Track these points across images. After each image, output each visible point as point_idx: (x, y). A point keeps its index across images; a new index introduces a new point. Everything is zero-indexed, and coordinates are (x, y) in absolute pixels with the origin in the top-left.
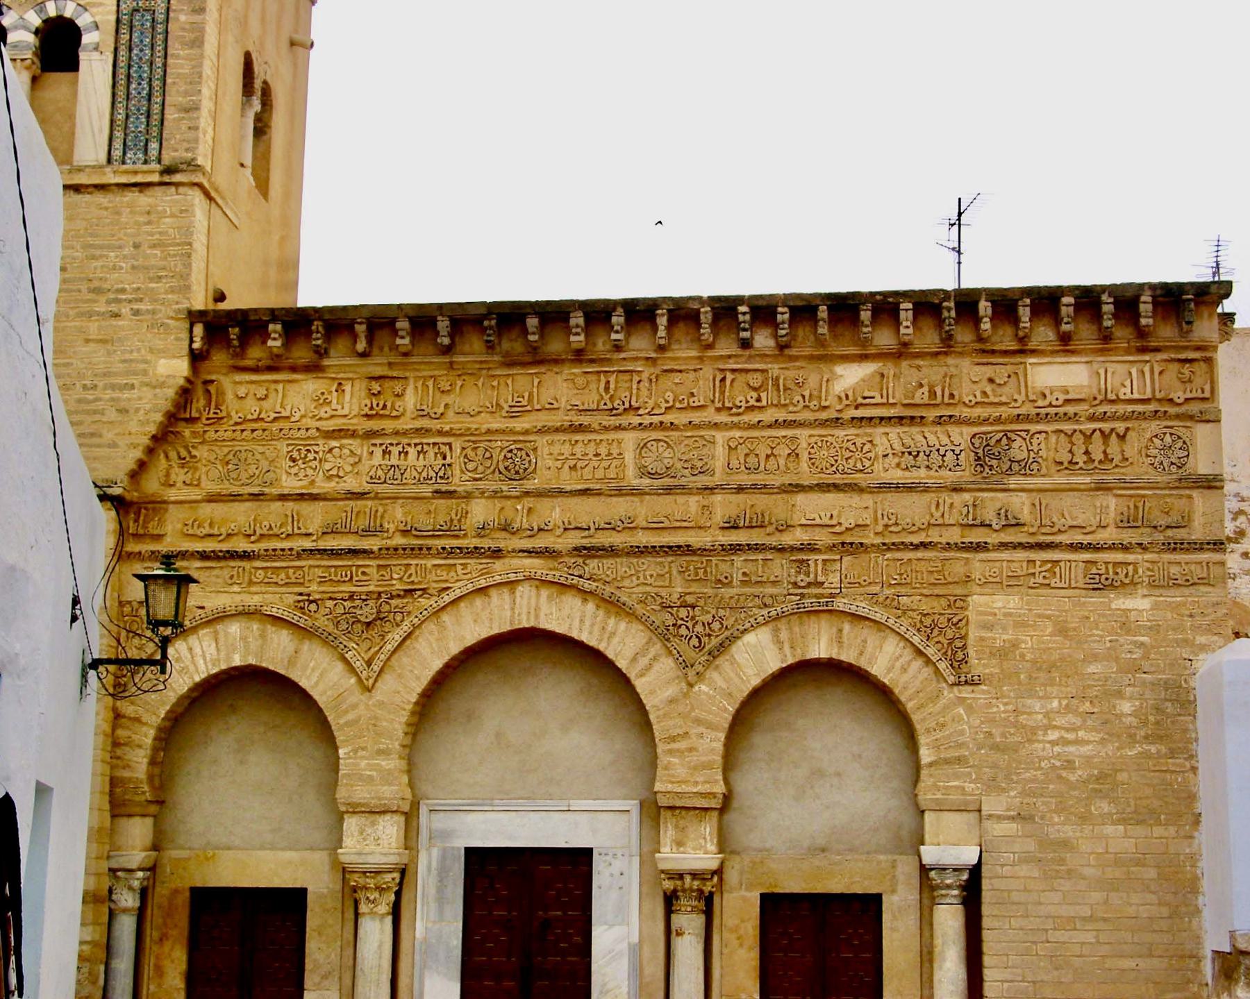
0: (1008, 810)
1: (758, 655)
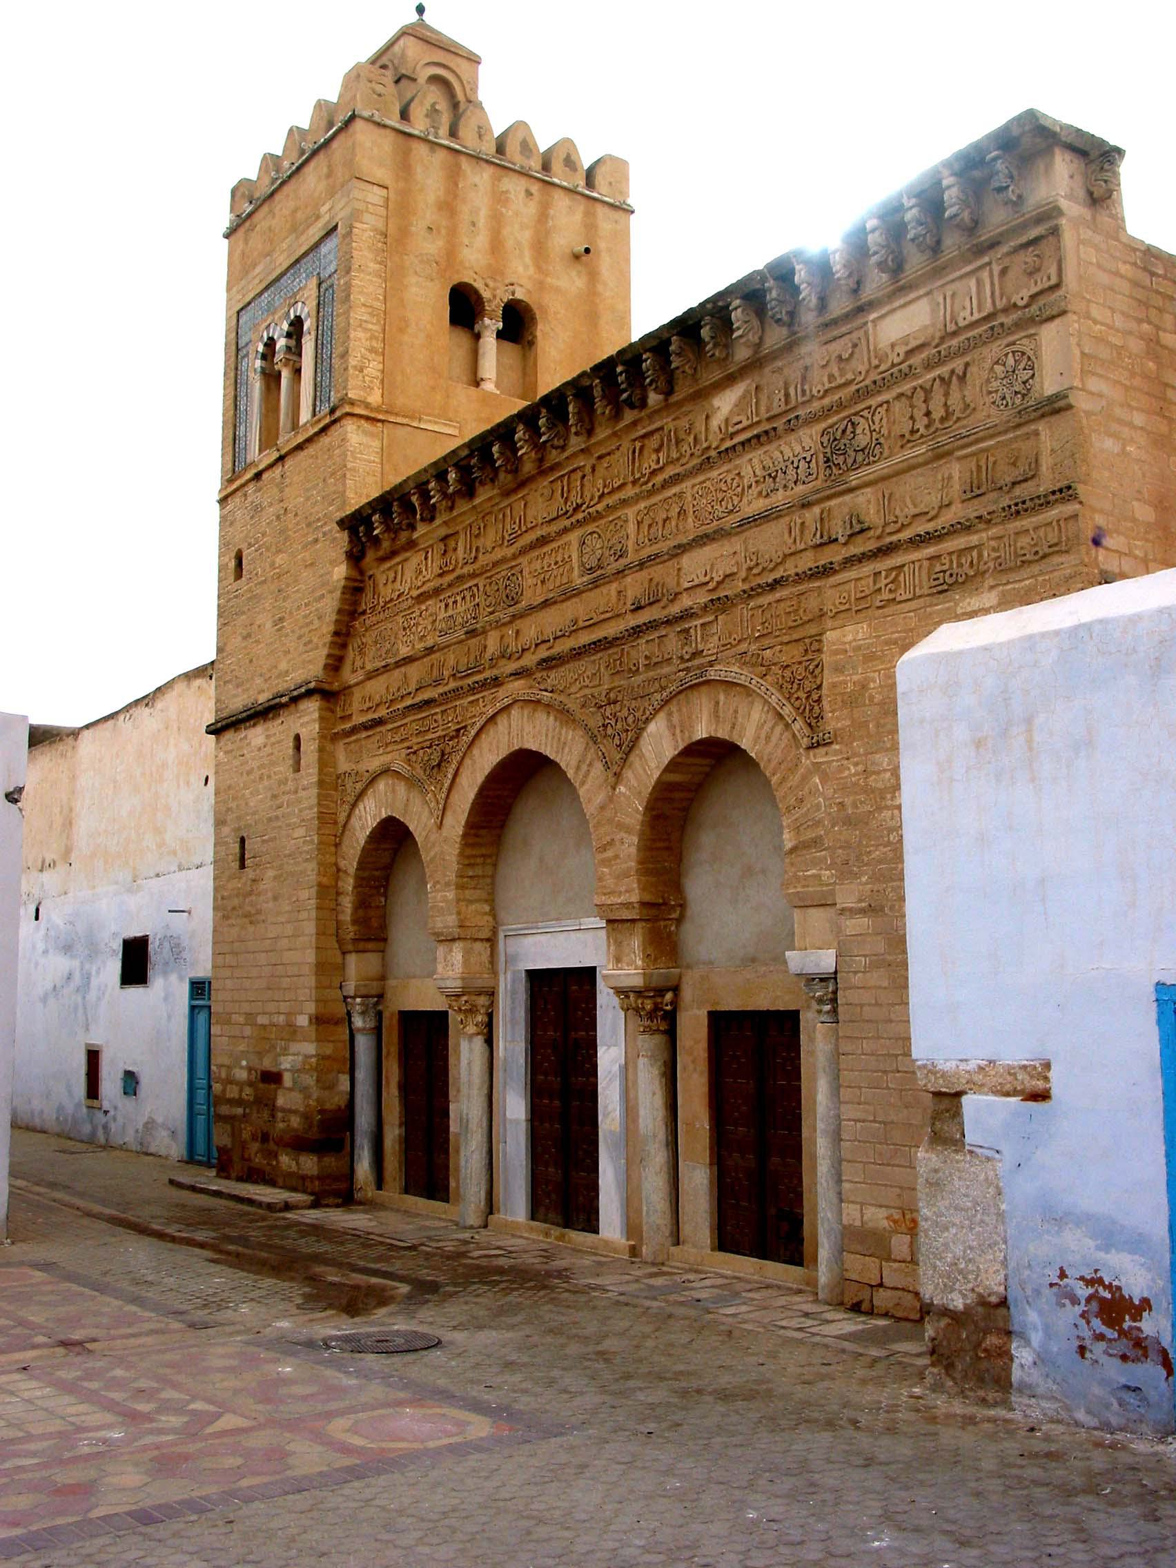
0: (860, 901)
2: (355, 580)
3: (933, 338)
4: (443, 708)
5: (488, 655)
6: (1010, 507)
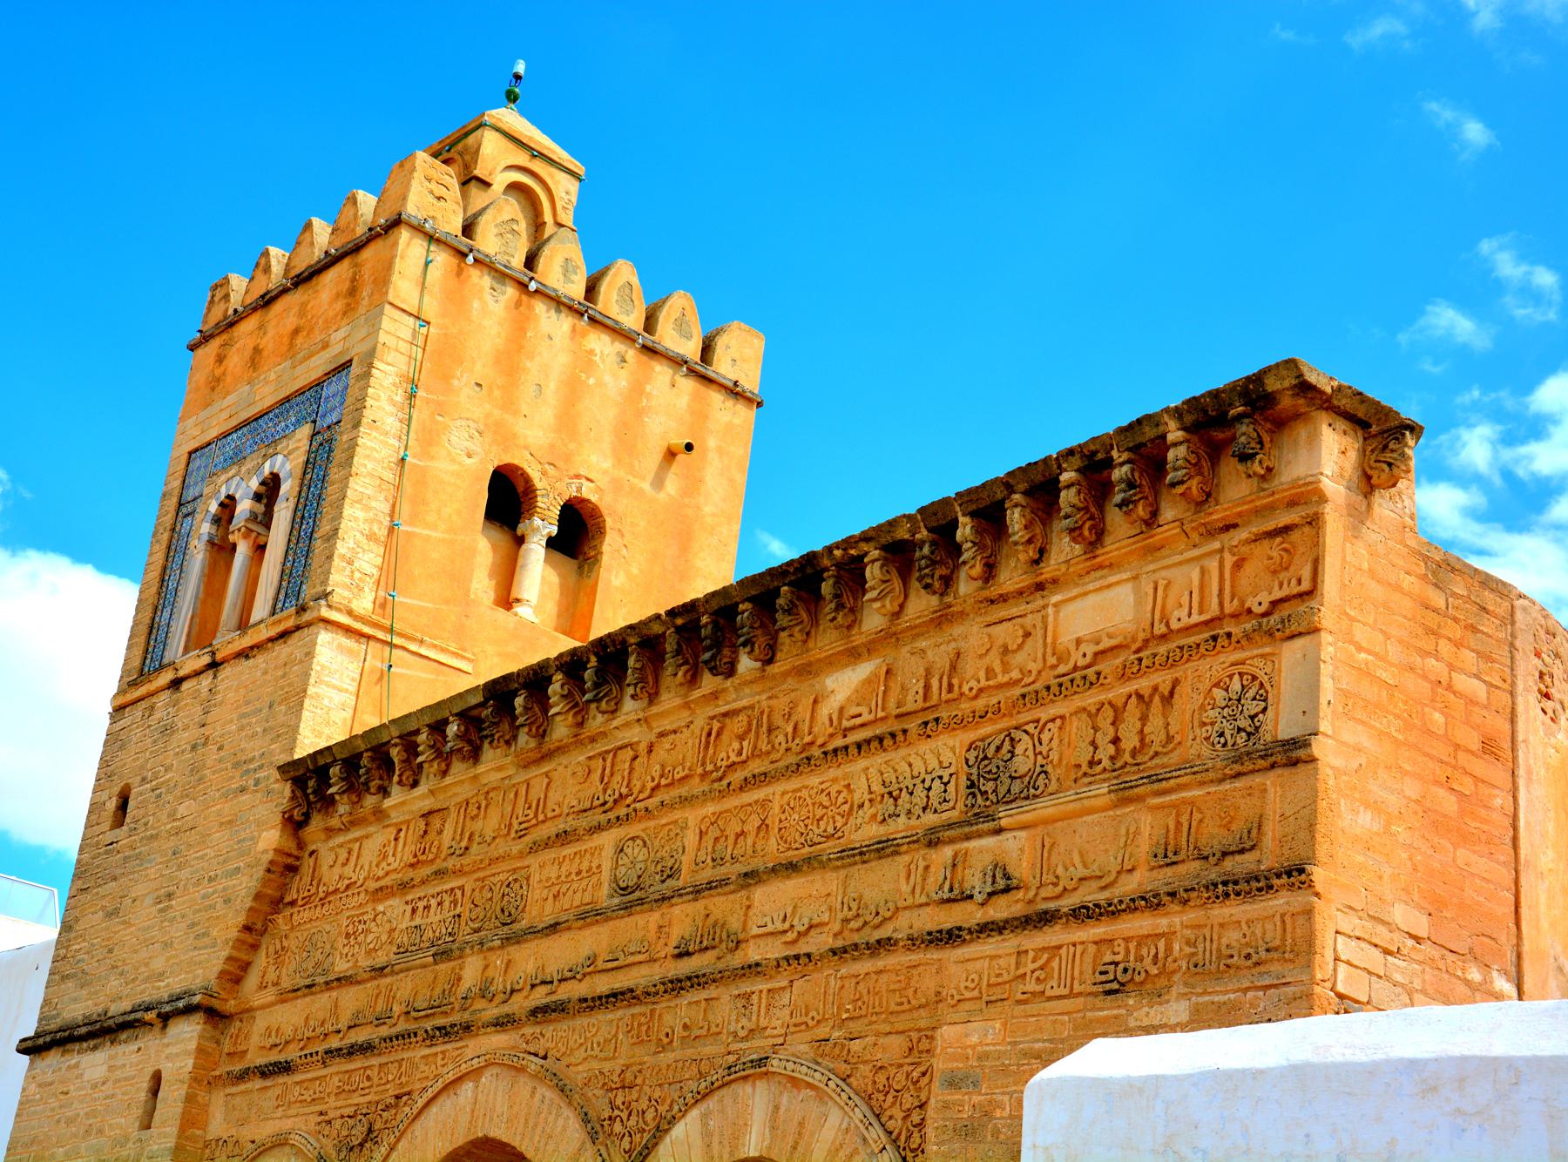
2: (290, 855)
3: (1134, 640)
4: (383, 1059)
5: (462, 990)
6: (1216, 885)
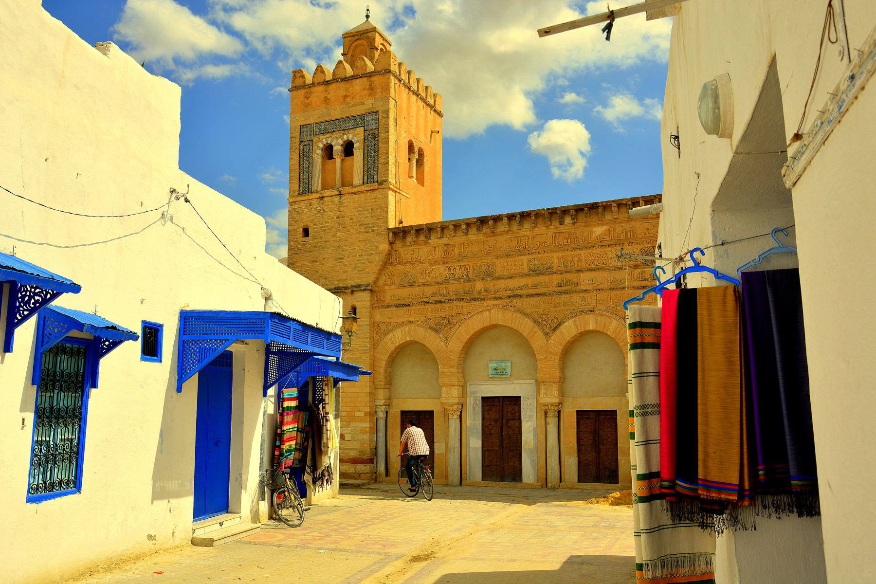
1: (569, 329)
